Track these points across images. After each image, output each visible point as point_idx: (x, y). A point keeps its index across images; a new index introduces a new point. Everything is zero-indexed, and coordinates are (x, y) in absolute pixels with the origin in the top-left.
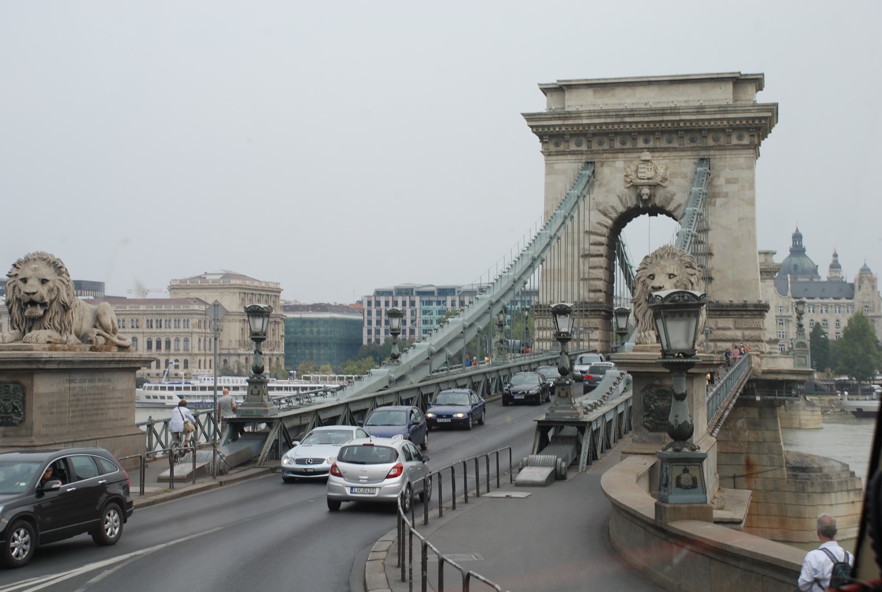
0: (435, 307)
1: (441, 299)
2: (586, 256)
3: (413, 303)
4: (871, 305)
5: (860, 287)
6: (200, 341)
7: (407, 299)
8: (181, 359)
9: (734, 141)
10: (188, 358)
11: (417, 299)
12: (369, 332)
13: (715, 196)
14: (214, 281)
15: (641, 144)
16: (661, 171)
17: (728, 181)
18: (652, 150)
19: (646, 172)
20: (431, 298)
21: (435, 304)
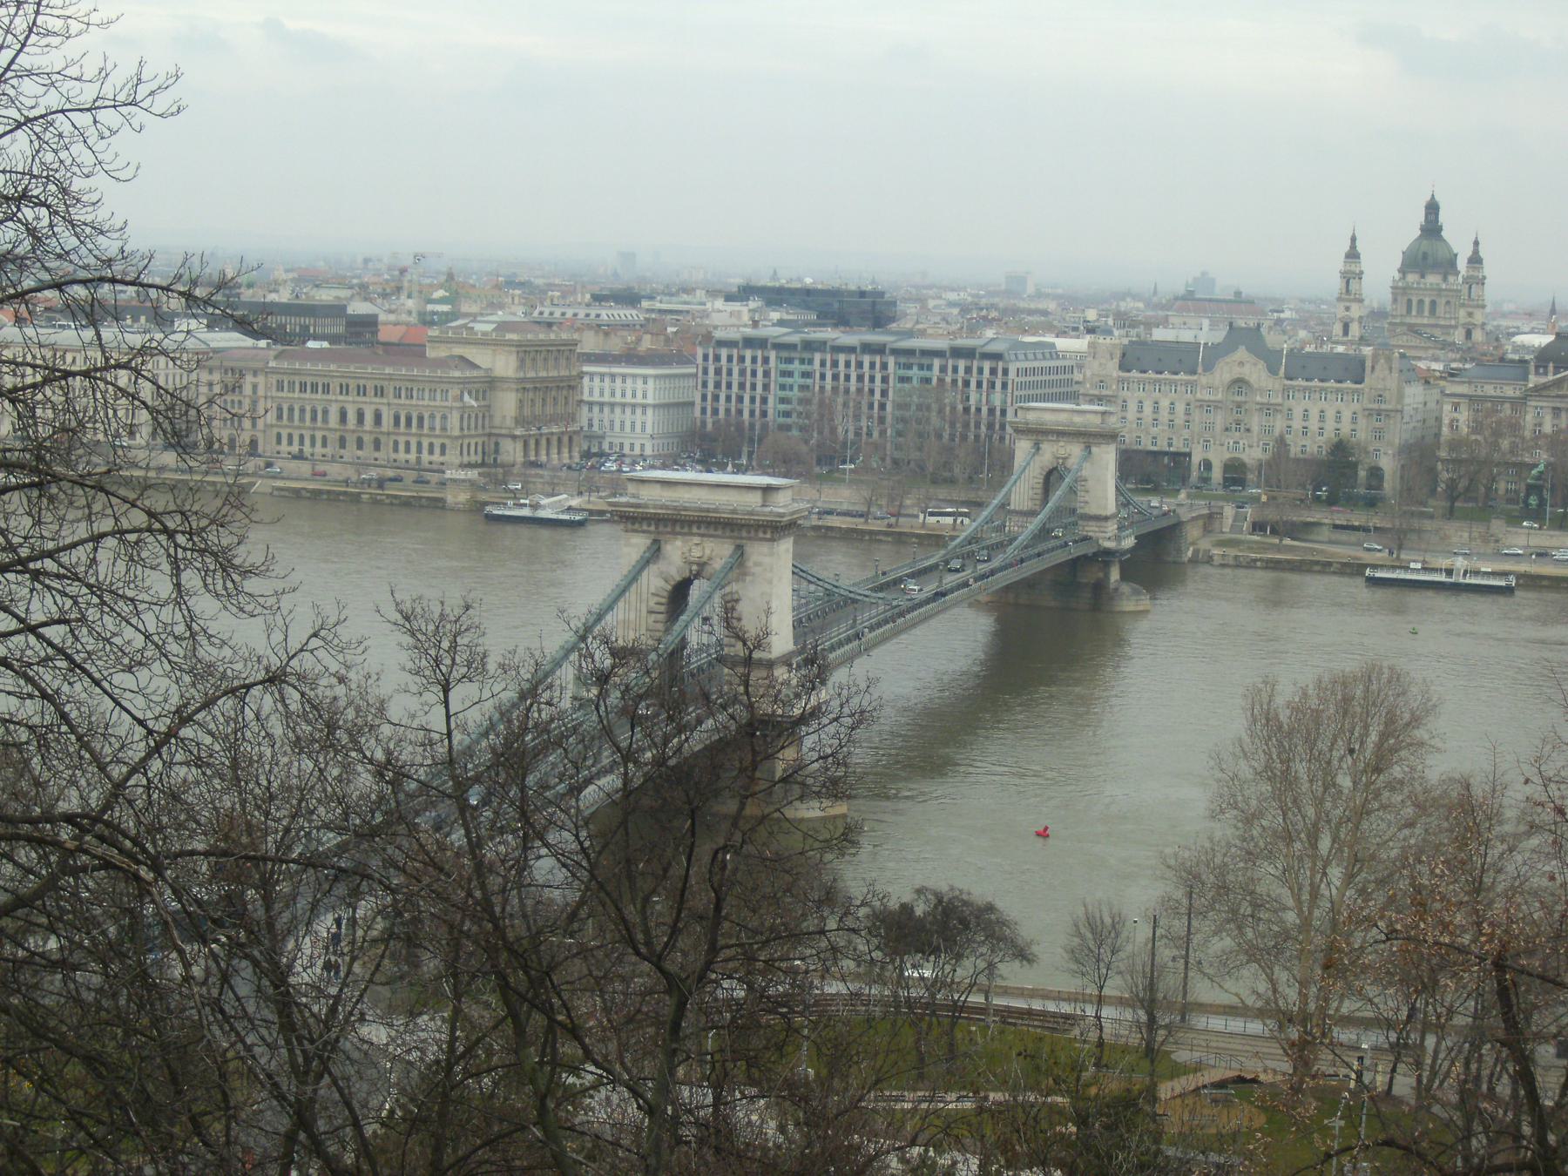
0: (796, 366)
1: (806, 355)
2: (650, 612)
3: (766, 360)
4: (1387, 395)
5: (1373, 368)
6: (462, 418)
7: (759, 353)
8: (437, 442)
9: (761, 535)
11: (773, 355)
12: (704, 398)
13: (745, 574)
14: (485, 334)
15: (695, 530)
16: (708, 552)
17: (757, 564)
18: (703, 535)
19: (696, 553)
20: (793, 355)
21: (797, 362)
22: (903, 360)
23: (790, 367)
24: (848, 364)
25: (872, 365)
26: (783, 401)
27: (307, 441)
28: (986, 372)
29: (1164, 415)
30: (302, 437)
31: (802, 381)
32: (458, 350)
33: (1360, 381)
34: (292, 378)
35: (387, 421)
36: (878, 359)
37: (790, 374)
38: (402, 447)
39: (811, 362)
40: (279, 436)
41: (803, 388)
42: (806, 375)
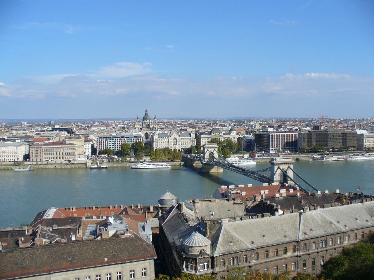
1: (113, 139)
7: (106, 139)
8: (73, 156)
10: (75, 156)
22: (127, 138)
23: (111, 141)
24: (119, 140)
25: (123, 140)
26: (110, 146)
27: (50, 158)
28: (140, 139)
29: (165, 143)
30: (49, 157)
31: (112, 143)
32: (71, 142)
33: (191, 136)
34: (47, 148)
35: (64, 154)
36: (124, 139)
37: (111, 142)
38: (67, 158)
39: (114, 140)
40: (45, 157)
41: (112, 144)
42: (113, 142)
